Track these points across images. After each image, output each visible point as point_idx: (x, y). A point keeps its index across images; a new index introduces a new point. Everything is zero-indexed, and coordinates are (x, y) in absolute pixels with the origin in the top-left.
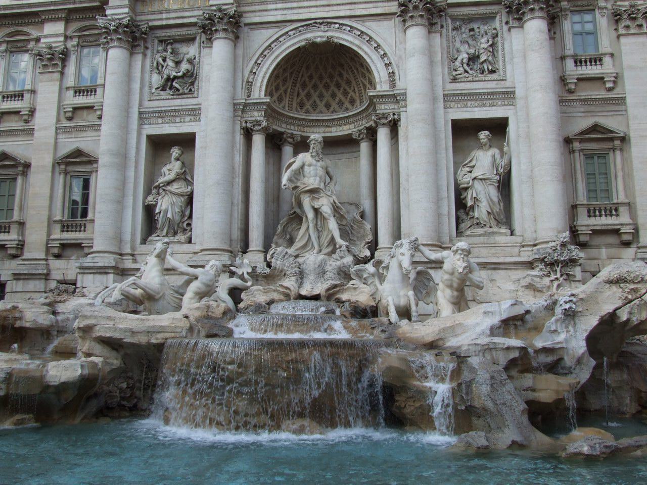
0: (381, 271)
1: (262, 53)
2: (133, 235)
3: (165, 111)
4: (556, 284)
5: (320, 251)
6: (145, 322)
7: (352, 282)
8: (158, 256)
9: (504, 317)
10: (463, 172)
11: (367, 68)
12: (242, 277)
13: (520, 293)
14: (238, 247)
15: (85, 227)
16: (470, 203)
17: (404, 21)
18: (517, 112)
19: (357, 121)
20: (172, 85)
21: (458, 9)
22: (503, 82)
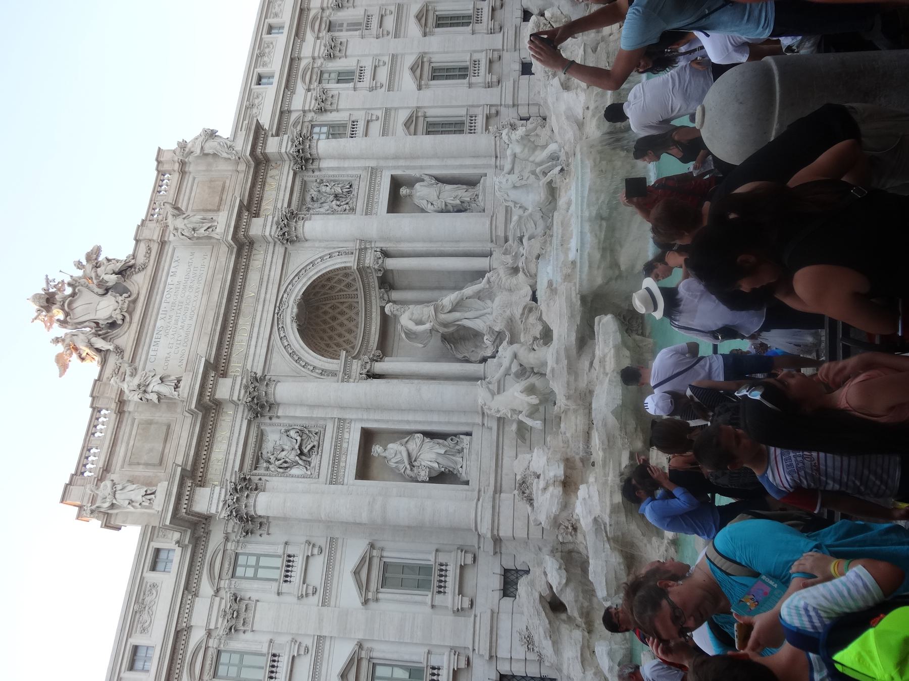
3: (334, 456)
7: (520, 265)
8: (493, 395)
15: (441, 565)
16: (458, 202)
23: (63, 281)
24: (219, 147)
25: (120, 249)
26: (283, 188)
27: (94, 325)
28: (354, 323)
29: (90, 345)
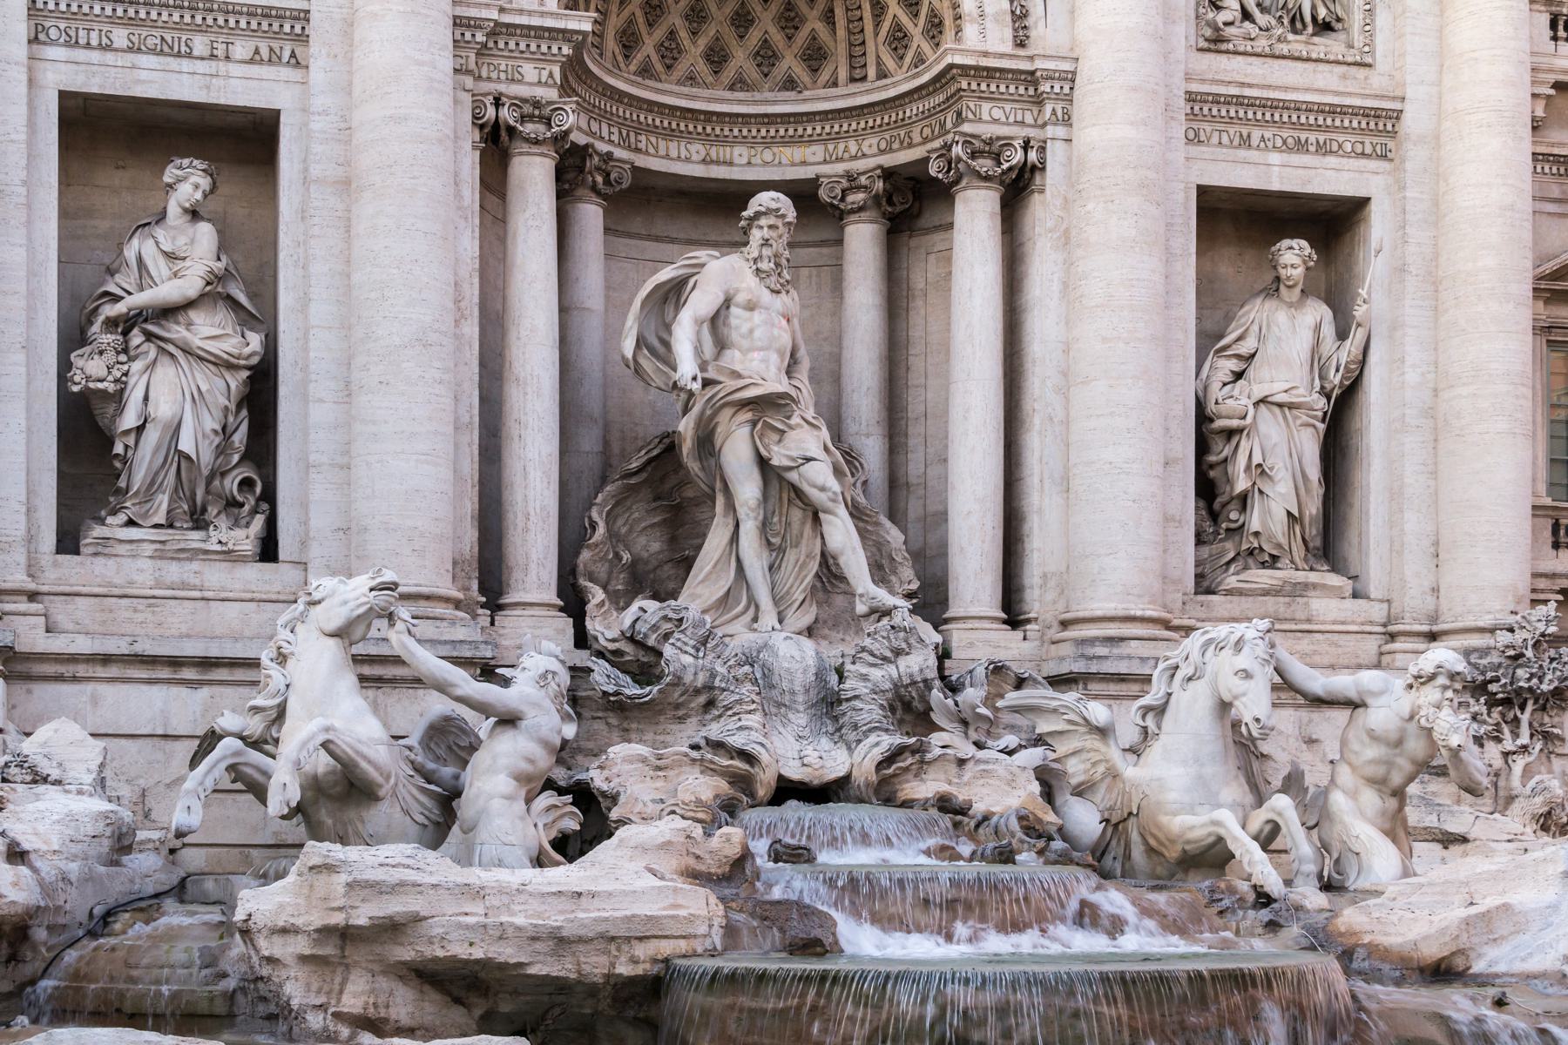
2: (30, 511)
6: (583, 899)
18: (1403, 188)
19: (838, 137)
22: (1361, 73)
28: (752, 73)
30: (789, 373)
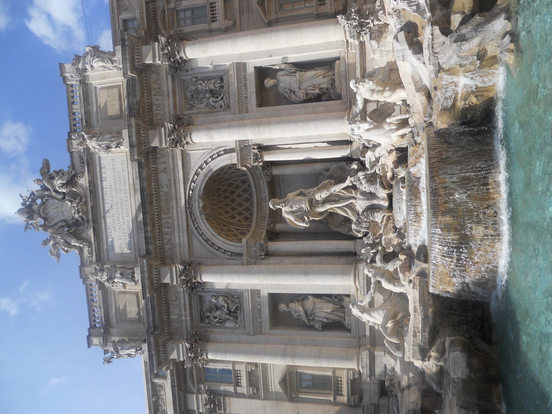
0: (371, 146)
1: (211, 246)
4: (376, 23)
5: (354, 197)
7: (378, 172)
9: (407, 47)
10: (295, 97)
11: (220, 170)
12: (375, 254)
13: (383, 49)
14: (351, 259)
16: (317, 91)
17: (187, 143)
20: (233, 312)
21: (178, 106)
23: (33, 192)
24: (104, 64)
25: (61, 162)
26: (166, 93)
27: (63, 224)
29: (68, 244)
30: (304, 195)
